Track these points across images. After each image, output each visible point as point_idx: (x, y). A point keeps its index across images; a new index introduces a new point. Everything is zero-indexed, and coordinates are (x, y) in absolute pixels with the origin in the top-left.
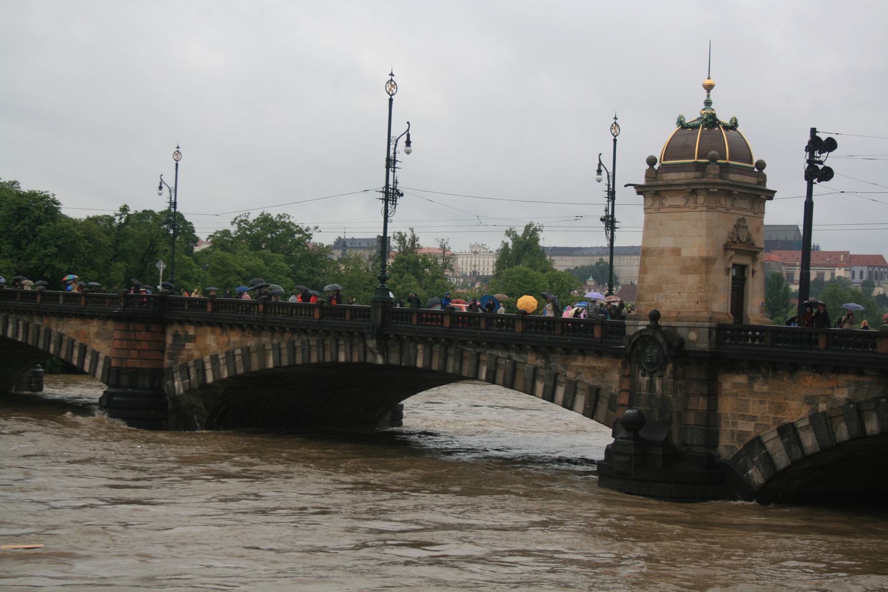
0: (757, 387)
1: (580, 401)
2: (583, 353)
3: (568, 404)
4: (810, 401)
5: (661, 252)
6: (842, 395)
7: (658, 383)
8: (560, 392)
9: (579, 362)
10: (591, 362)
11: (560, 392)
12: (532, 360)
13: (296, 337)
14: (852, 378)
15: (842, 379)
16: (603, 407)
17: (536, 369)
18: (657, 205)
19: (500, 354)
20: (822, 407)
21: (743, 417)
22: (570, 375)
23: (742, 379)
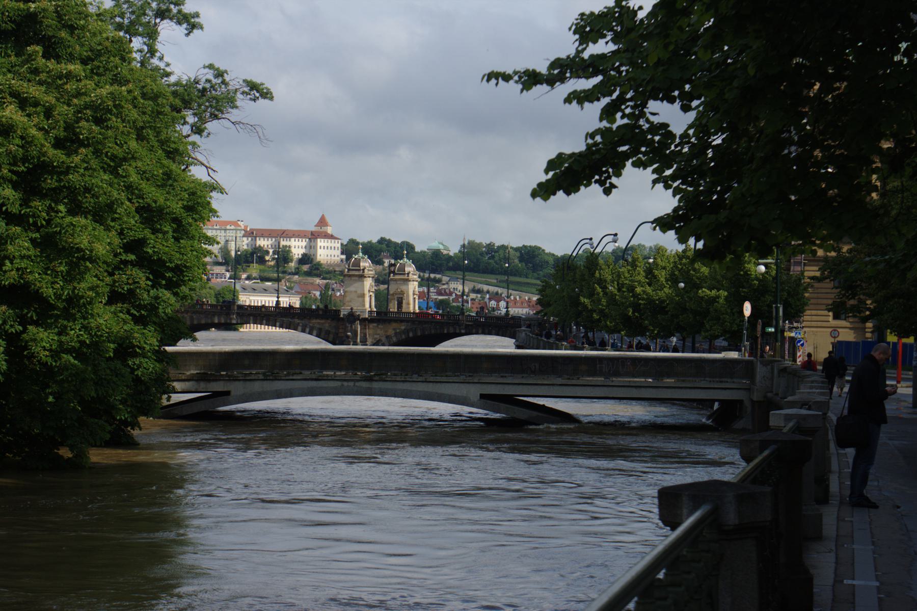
0: (379, 326)
1: (315, 333)
2: (316, 318)
3: (310, 333)
4: (394, 329)
5: (351, 292)
6: (403, 328)
7: (353, 326)
8: (308, 330)
9: (314, 321)
10: (318, 321)
11: (308, 330)
12: (297, 321)
13: (193, 315)
14: (405, 324)
15: (403, 324)
16: (323, 334)
17: (299, 323)
18: (349, 279)
19: (284, 319)
20: (398, 331)
21: (376, 334)
22: (311, 325)
23: (375, 325)
